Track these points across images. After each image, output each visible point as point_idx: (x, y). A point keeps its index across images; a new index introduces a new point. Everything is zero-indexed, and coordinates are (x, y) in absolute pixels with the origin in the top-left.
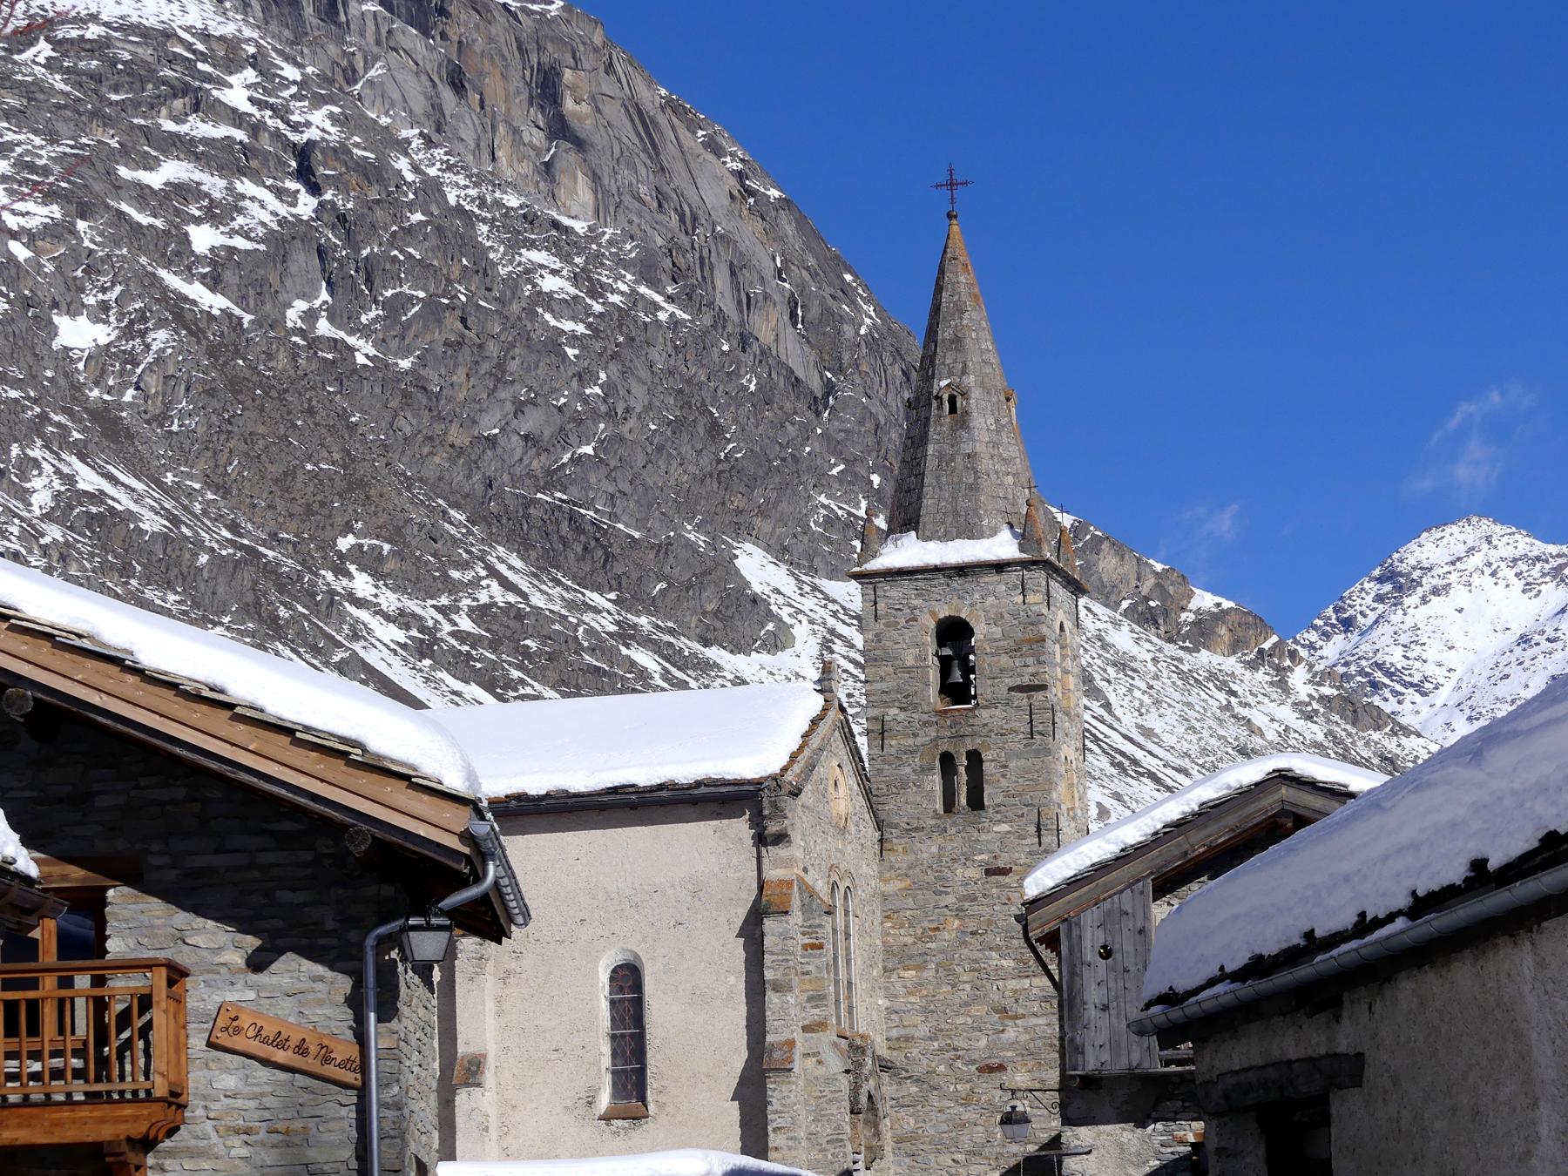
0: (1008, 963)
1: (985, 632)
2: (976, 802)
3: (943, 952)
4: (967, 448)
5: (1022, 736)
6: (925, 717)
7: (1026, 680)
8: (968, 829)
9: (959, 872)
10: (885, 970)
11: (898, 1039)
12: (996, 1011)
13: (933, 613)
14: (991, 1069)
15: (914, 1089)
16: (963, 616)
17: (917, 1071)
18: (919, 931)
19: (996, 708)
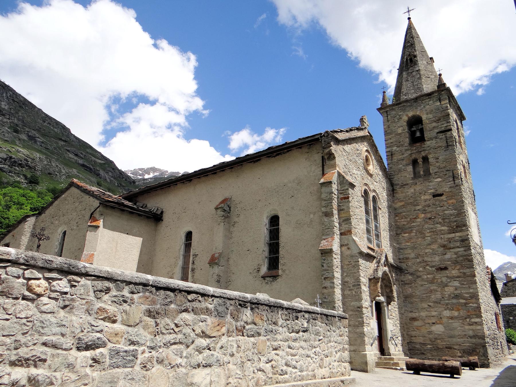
0: (445, 228)
1: (426, 117)
2: (427, 173)
3: (418, 226)
4: (417, 69)
5: (443, 148)
6: (407, 148)
7: (443, 129)
8: (425, 182)
9: (422, 197)
10: (397, 234)
11: (403, 259)
12: (442, 247)
13: (407, 115)
14: (441, 269)
15: (410, 277)
16: (418, 114)
17: (411, 270)
18: (409, 219)
19: (432, 140)
